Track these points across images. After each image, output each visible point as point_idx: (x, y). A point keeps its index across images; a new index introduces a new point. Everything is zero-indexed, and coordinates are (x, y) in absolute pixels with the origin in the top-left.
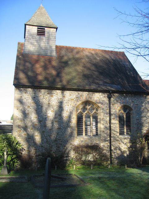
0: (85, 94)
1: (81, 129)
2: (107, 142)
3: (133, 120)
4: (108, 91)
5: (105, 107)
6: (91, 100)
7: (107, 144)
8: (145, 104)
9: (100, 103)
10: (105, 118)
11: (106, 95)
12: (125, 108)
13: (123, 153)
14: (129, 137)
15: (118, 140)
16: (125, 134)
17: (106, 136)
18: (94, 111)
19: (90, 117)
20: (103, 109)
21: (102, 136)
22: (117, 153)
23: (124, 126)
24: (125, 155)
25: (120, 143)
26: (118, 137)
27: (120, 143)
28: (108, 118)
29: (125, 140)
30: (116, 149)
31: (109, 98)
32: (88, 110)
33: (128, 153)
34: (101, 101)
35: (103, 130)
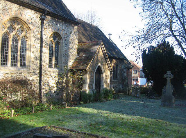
0: (15, 7)
1: (6, 63)
2: (36, 76)
3: (62, 52)
4: (42, 11)
5: (36, 30)
6: (21, 18)
7: (36, 78)
8: (73, 34)
9: (31, 24)
10: (35, 44)
11: (39, 16)
12: (56, 36)
13: (50, 89)
14: (58, 71)
15: (47, 74)
16: (53, 66)
17: (36, 68)
18: (24, 33)
19: (17, 41)
20: (34, 33)
21: (31, 68)
22: (45, 90)
23: (52, 57)
24: (53, 92)
25: (48, 78)
26: (47, 70)
27: (48, 78)
28: (39, 45)
29: (54, 74)
30: (44, 85)
31: (42, 20)
32: (16, 31)
33: (55, 89)
34: (33, 22)
35: (32, 59)
